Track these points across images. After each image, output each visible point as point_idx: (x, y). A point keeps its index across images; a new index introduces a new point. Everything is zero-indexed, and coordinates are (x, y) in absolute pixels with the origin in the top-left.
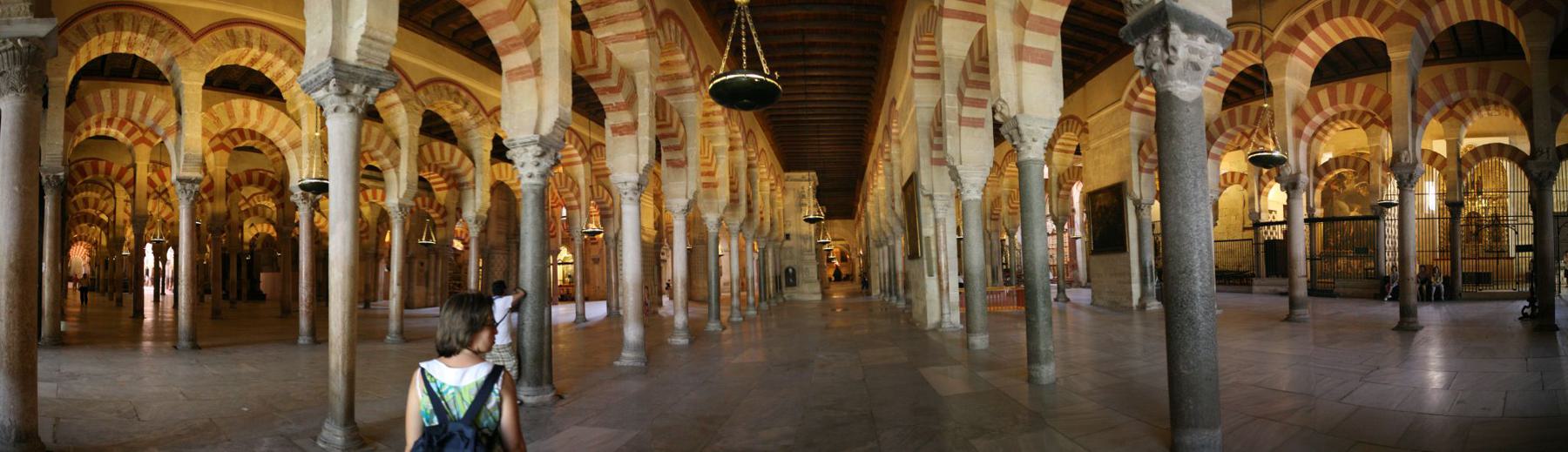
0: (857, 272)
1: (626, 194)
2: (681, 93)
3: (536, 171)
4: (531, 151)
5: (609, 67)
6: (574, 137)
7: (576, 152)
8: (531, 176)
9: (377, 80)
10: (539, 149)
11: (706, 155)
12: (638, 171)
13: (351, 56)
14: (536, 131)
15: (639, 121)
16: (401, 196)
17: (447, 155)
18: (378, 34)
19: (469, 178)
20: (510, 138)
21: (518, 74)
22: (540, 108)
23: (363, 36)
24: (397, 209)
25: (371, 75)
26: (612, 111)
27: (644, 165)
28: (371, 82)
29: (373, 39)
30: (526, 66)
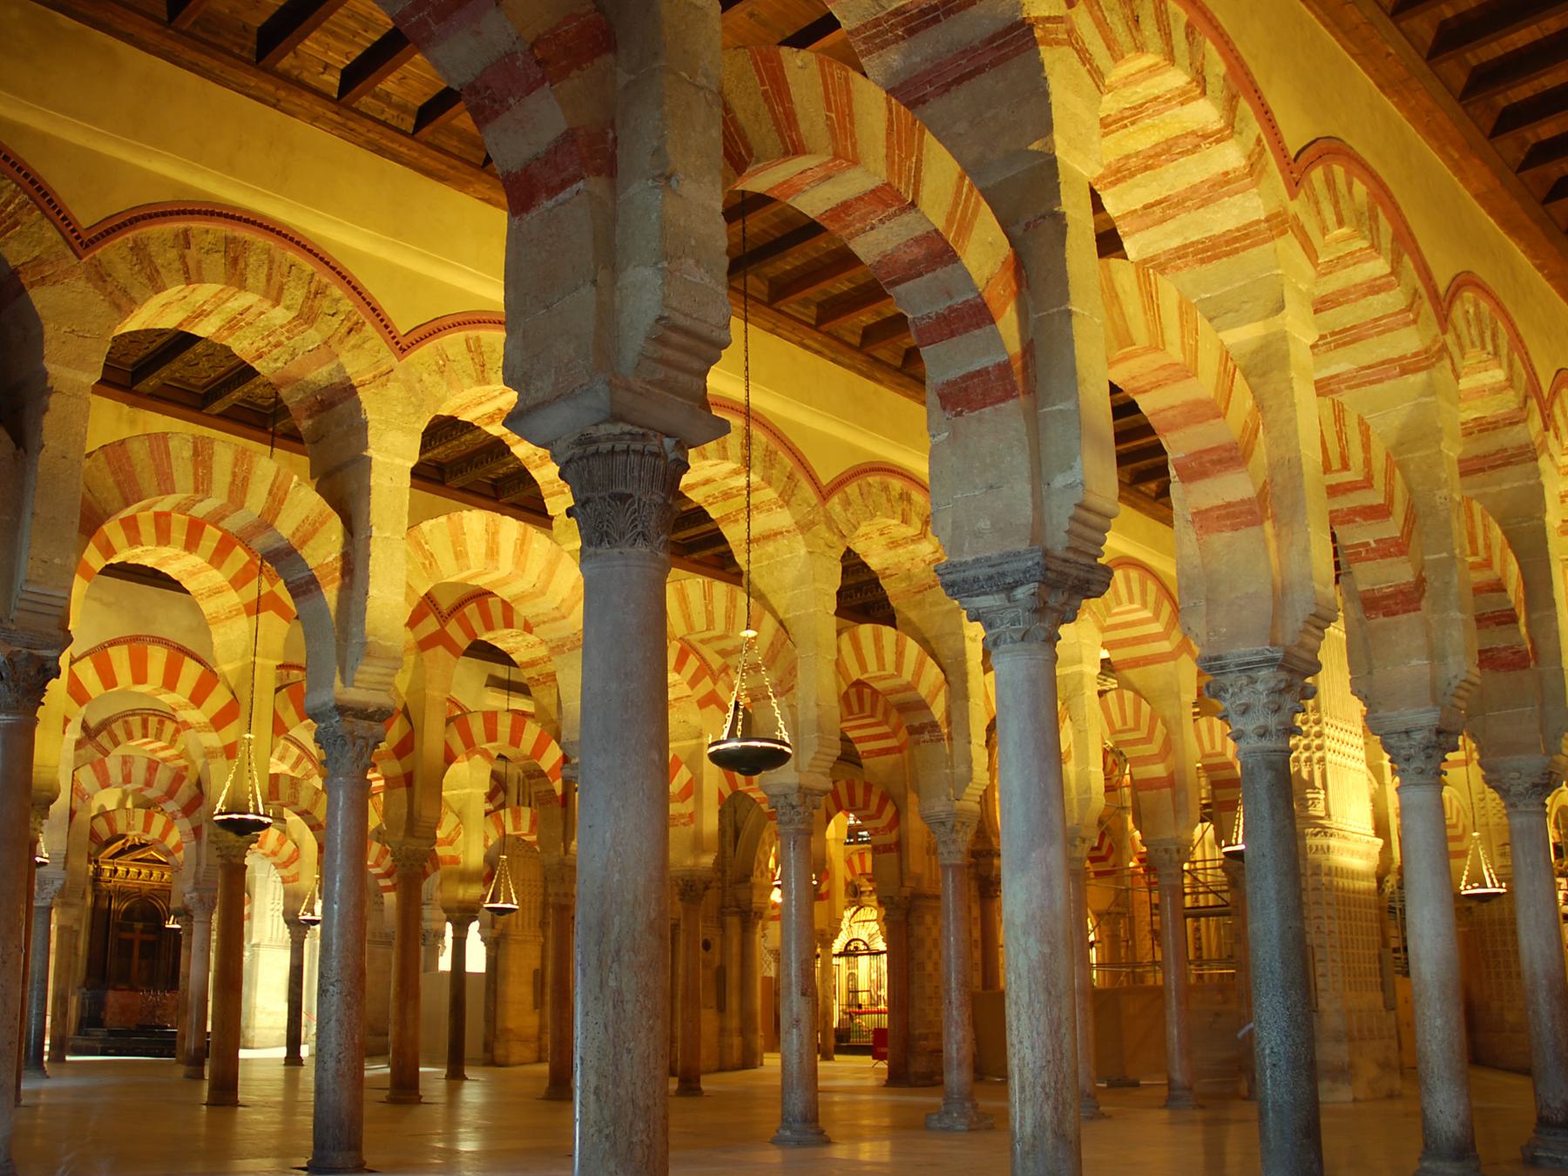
17: (890, 657)
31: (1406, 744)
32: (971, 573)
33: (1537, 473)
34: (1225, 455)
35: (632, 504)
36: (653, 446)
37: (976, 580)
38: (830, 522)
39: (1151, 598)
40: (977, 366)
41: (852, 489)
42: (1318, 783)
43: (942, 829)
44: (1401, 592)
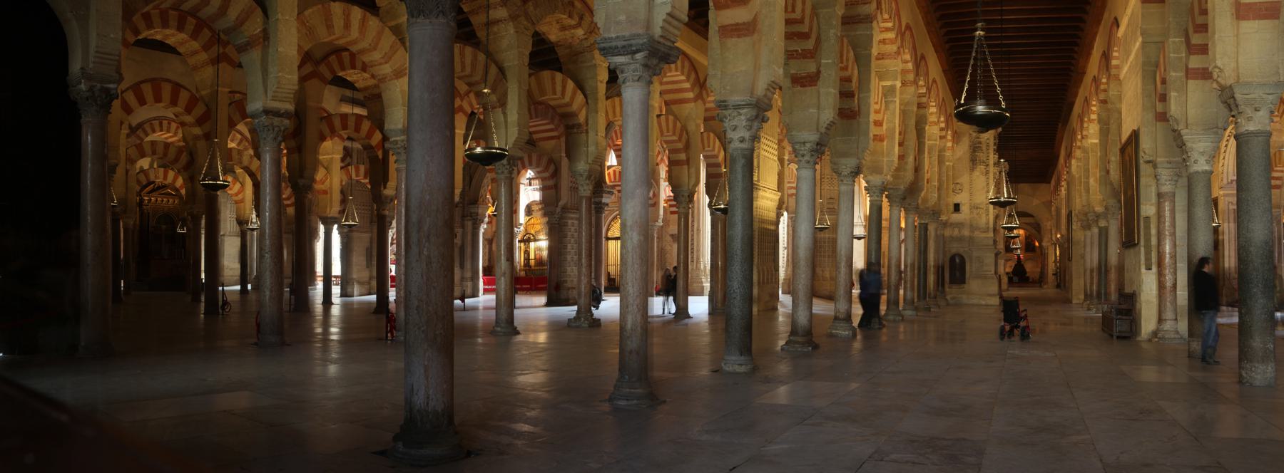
0: (1051, 267)
1: (803, 156)
2: (854, 23)
4: (745, 115)
6: (687, 64)
7: (687, 85)
11: (876, 101)
12: (818, 131)
15: (822, 69)
17: (559, 88)
19: (582, 118)
26: (796, 58)
27: (828, 122)
31: (803, 149)
32: (614, 44)
33: (872, 28)
37: (616, 47)
39: (686, 70)
43: (581, 178)
44: (810, 77)
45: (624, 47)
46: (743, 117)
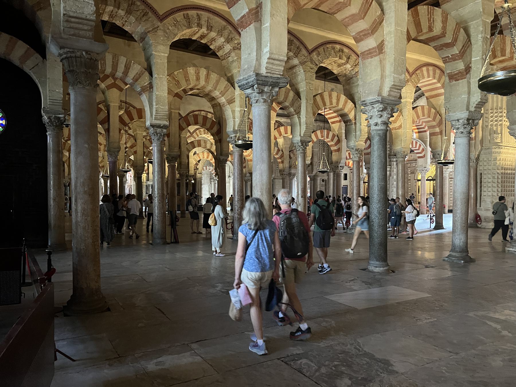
3: (379, 121)
5: (444, 28)
8: (376, 124)
9: (277, 82)
10: (381, 106)
13: (263, 71)
14: (379, 95)
15: (473, 65)
16: (302, 135)
17: (334, 101)
18: (276, 57)
20: (363, 100)
21: (367, 54)
22: (383, 77)
23: (269, 58)
24: (300, 144)
25: (274, 81)
27: (477, 103)
28: (274, 85)
29: (274, 59)
30: (373, 48)
31: (457, 124)
34: (366, 32)
35: (75, 73)
36: (78, 54)
38: (312, 61)
39: (437, 76)
40: (242, 14)
41: (321, 49)
42: (499, 132)
43: (353, 150)
45: (246, 84)
46: (375, 110)
